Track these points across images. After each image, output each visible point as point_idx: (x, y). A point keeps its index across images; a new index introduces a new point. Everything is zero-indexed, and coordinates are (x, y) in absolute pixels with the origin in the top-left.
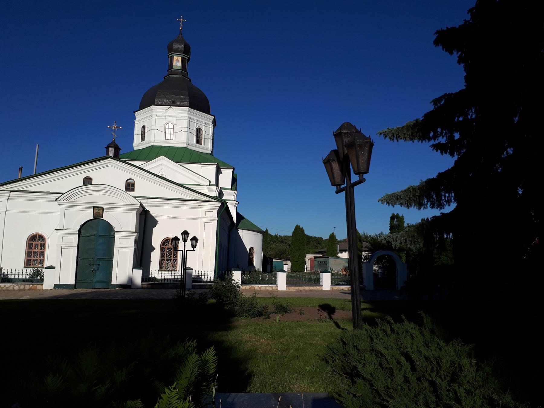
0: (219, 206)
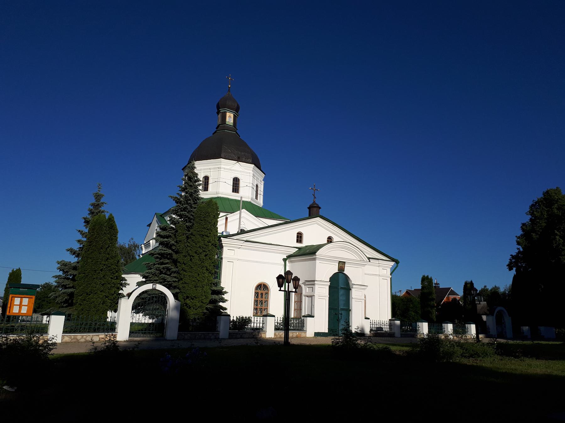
0: (393, 265)
